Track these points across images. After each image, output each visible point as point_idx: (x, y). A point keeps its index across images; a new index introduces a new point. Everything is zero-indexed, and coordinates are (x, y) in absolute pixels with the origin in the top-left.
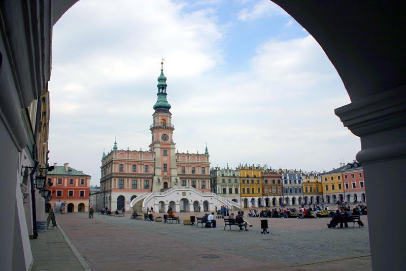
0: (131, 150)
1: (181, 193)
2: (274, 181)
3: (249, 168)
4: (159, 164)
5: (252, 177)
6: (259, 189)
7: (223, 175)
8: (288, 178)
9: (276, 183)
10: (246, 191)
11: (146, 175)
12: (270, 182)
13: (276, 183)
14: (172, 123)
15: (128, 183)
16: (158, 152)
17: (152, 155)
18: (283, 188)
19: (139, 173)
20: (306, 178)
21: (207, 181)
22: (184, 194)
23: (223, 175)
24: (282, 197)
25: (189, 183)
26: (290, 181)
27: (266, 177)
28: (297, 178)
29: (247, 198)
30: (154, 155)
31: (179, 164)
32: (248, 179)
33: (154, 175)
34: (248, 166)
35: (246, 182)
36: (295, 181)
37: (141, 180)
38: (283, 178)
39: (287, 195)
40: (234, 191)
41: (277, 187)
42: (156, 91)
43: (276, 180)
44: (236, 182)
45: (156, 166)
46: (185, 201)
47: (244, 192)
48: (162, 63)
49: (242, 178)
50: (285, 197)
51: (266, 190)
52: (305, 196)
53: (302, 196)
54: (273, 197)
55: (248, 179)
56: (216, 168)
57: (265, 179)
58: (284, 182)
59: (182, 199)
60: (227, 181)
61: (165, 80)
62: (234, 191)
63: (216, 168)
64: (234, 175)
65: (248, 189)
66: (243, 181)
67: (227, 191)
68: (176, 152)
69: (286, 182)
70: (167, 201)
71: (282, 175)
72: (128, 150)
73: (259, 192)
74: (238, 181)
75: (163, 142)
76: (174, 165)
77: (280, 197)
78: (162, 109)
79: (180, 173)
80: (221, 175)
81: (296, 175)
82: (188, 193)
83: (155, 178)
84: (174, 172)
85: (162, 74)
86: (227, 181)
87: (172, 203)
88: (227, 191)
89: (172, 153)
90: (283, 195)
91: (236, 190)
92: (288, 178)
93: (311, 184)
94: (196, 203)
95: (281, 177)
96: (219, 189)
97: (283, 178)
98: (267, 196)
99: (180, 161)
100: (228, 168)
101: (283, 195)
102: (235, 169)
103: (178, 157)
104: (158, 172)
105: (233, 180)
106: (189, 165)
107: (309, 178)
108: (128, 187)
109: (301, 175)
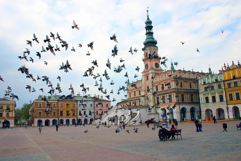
11: (135, 97)
32: (235, 81)
35: (232, 85)
40: (218, 99)
44: (220, 86)
48: (147, 11)
49: (226, 81)
55: (235, 81)
61: (151, 23)
62: (218, 99)
66: (229, 84)
67: (210, 100)
74: (222, 86)
80: (203, 84)
85: (148, 19)
88: (210, 100)
91: (221, 99)
96: (201, 98)
102: (219, 72)
105: (216, 86)
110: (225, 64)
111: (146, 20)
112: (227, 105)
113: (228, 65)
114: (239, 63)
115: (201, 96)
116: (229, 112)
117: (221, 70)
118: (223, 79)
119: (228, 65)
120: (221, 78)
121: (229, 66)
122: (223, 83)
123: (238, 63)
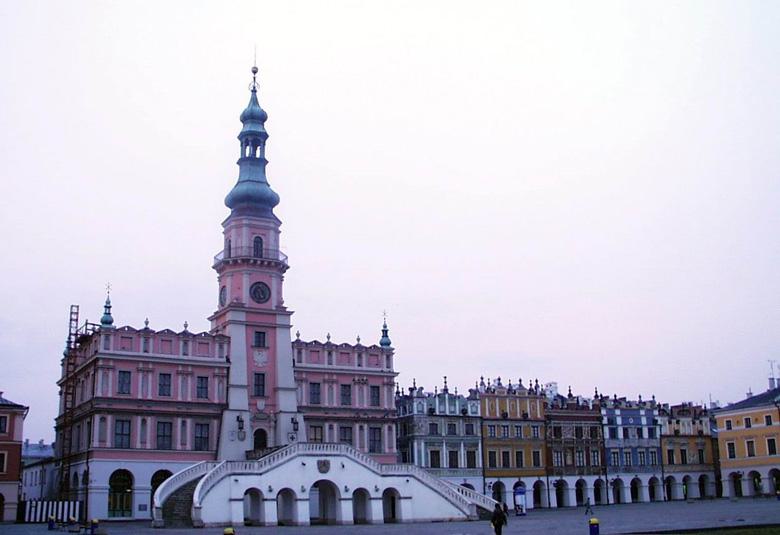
0: (156, 327)
1: (312, 462)
2: (579, 431)
3: (510, 390)
4: (239, 374)
5: (516, 420)
6: (536, 454)
7: (431, 411)
8: (619, 421)
12: (568, 434)
14: (280, 249)
15: (144, 431)
16: (239, 337)
17: (221, 347)
18: (604, 451)
19: (180, 399)
20: (670, 423)
21: (386, 427)
22: (324, 467)
23: (431, 411)
24: (603, 478)
25: (332, 432)
27: (557, 418)
28: (644, 421)
29: (501, 480)
30: (225, 346)
31: (299, 372)
33: (225, 406)
34: (505, 384)
37: (184, 423)
38: (605, 421)
41: (587, 450)
42: (235, 150)
43: (586, 426)
44: (469, 431)
45: (232, 382)
46: (326, 491)
47: (493, 464)
48: (255, 72)
50: (611, 477)
51: (556, 459)
52: (666, 476)
53: (659, 476)
54: (578, 478)
56: (411, 390)
57: (553, 423)
59: (316, 484)
60: (444, 431)
63: (411, 390)
64: (464, 411)
65: (506, 454)
68: (294, 338)
69: (613, 434)
70: (271, 491)
71: (603, 412)
72: (146, 329)
73: (537, 464)
74: (477, 430)
75: (255, 305)
76: (285, 376)
77: (597, 477)
78: (252, 205)
79: (304, 404)
80: (425, 410)
81: (642, 412)
82: (334, 462)
83: (229, 419)
84: (287, 402)
85: (254, 101)
86: (444, 431)
87: (287, 495)
89: (283, 343)
90: (605, 473)
92: (619, 421)
93: (683, 441)
94: (361, 496)
95: (600, 419)
96: (419, 452)
97: (605, 421)
98: (560, 474)
99: (304, 364)
101: (605, 473)
102: (468, 394)
103: (300, 353)
104: (239, 400)
106: (331, 376)
107: (678, 422)
108: (143, 442)
109: (656, 412)
110: (482, 378)
111: (244, 104)
112: (484, 478)
115: (419, 444)
118: (479, 415)
120: (474, 409)
122: (479, 424)
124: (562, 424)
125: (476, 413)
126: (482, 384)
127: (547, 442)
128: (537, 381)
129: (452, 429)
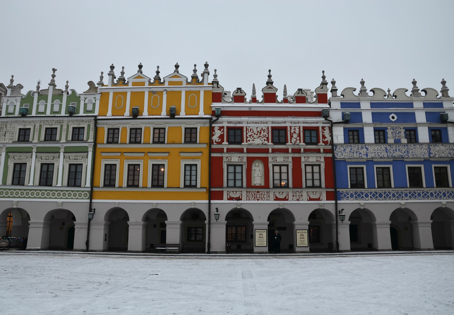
8: (367, 118)
9: (295, 141)
10: (122, 177)
13: (295, 141)
26: (381, 135)
28: (421, 117)
36: (412, 136)
38: (336, 116)
39: (359, 196)
47: (110, 182)
50: (349, 204)
58: (339, 135)
65: (133, 170)
69: (355, 136)
92: (367, 118)
97: (336, 116)
100: (52, 84)
110: (112, 67)
113: (123, 73)
114: (158, 72)
116: (92, 227)
117: (96, 81)
118: (96, 113)
119: (123, 73)
121: (125, 75)
123: (155, 74)
124: (244, 122)
125: (93, 111)
126: (111, 74)
127: (211, 151)
128: (206, 66)
129: (51, 134)
